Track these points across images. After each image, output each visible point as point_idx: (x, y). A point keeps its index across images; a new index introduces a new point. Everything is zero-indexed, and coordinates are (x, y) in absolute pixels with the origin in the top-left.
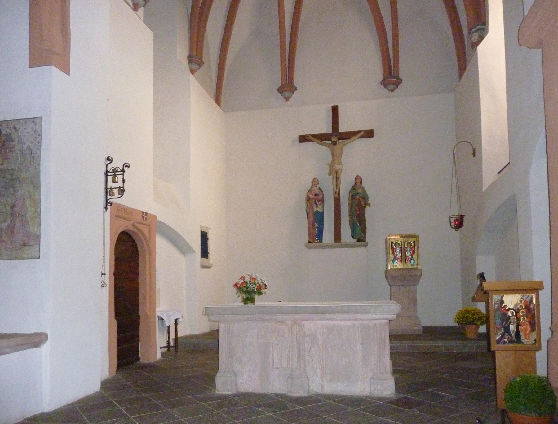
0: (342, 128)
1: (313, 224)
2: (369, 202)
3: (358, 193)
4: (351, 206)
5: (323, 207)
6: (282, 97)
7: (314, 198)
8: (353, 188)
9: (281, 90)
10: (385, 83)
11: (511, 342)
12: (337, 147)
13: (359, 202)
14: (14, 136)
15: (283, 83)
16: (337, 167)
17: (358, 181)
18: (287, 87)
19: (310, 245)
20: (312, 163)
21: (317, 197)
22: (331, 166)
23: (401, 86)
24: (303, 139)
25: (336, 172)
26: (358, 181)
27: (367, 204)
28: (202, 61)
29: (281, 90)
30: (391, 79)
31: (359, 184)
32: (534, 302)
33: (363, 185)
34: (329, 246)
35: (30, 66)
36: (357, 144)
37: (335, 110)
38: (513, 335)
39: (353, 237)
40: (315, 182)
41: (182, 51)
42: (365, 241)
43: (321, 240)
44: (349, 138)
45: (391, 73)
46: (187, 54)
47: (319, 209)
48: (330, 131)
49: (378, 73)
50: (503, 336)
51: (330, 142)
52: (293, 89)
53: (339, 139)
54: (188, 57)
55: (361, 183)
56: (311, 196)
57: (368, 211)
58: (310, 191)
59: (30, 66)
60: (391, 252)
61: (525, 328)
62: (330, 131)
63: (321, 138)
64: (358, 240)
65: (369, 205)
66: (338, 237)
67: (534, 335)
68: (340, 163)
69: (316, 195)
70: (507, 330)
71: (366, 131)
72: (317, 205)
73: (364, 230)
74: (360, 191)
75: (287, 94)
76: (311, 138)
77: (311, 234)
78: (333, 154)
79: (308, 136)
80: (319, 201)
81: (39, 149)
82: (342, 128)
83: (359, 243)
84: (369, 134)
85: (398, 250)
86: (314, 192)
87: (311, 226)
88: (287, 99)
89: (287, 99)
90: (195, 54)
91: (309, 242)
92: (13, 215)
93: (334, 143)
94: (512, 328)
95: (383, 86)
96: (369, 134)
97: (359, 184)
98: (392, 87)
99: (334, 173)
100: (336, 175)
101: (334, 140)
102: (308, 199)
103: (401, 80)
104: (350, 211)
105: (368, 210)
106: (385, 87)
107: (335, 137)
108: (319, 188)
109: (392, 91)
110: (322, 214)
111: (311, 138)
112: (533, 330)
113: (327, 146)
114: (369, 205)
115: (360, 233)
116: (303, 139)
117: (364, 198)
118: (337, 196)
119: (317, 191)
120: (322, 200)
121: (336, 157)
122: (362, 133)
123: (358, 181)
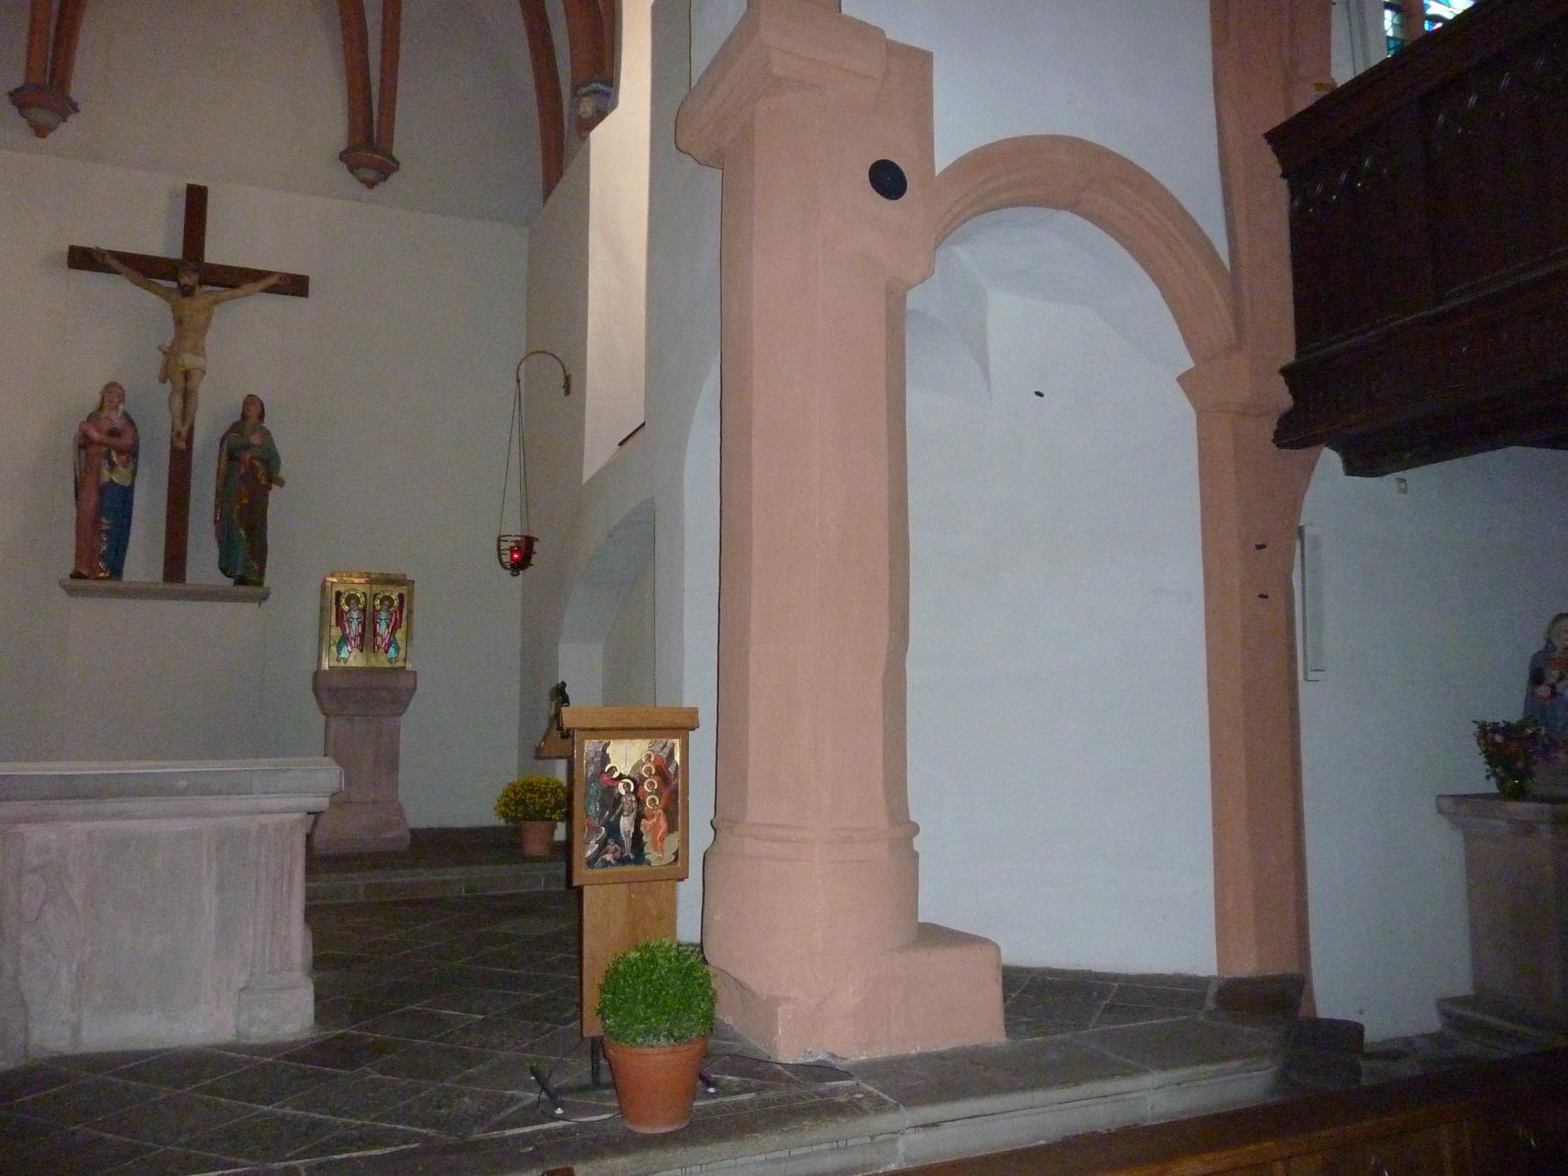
0: (217, 252)
1: (96, 522)
2: (282, 474)
3: (249, 447)
4: (224, 479)
5: (134, 474)
6: (24, 122)
7: (103, 443)
8: (236, 428)
9: (20, 100)
10: (351, 158)
11: (622, 861)
13: (250, 468)
16: (188, 360)
17: (253, 410)
19: (81, 583)
20: (112, 338)
21: (115, 441)
22: (170, 354)
23: (394, 178)
24: (82, 259)
25: (187, 375)
26: (254, 411)
27: (273, 479)
30: (369, 153)
31: (253, 420)
32: (677, 758)
33: (267, 423)
34: (140, 592)
36: (259, 307)
38: (628, 843)
39: (224, 570)
40: (112, 393)
42: (260, 584)
43: (116, 571)
44: (233, 286)
47: (120, 477)
48: (176, 252)
49: (334, 129)
50: (603, 845)
51: (174, 285)
53: (203, 282)
55: (261, 417)
56: (95, 435)
58: (93, 418)
60: (334, 622)
61: (655, 823)
62: (176, 252)
63: (143, 268)
64: (241, 581)
65: (281, 483)
67: (673, 842)
68: (199, 351)
69: (114, 433)
70: (613, 830)
72: (112, 466)
73: (258, 552)
74: (255, 439)
78: (179, 322)
80: (120, 452)
82: (217, 252)
83: (242, 589)
84: (296, 286)
85: (355, 615)
86: (106, 425)
87: (85, 531)
88: (41, 131)
91: (76, 575)
93: (187, 292)
94: (626, 824)
96: (296, 286)
97: (253, 420)
98: (370, 175)
99: (180, 379)
100: (183, 385)
101: (185, 280)
102: (84, 443)
103: (398, 163)
104: (221, 496)
105: (275, 496)
106: (352, 169)
107: (188, 273)
108: (126, 416)
109: (371, 185)
110: (127, 493)
112: (672, 828)
113: (166, 295)
114: (281, 483)
115: (245, 561)
116: (82, 259)
117: (266, 462)
118: (182, 445)
120: (132, 453)
121: (187, 333)
122: (272, 281)
123: (253, 410)
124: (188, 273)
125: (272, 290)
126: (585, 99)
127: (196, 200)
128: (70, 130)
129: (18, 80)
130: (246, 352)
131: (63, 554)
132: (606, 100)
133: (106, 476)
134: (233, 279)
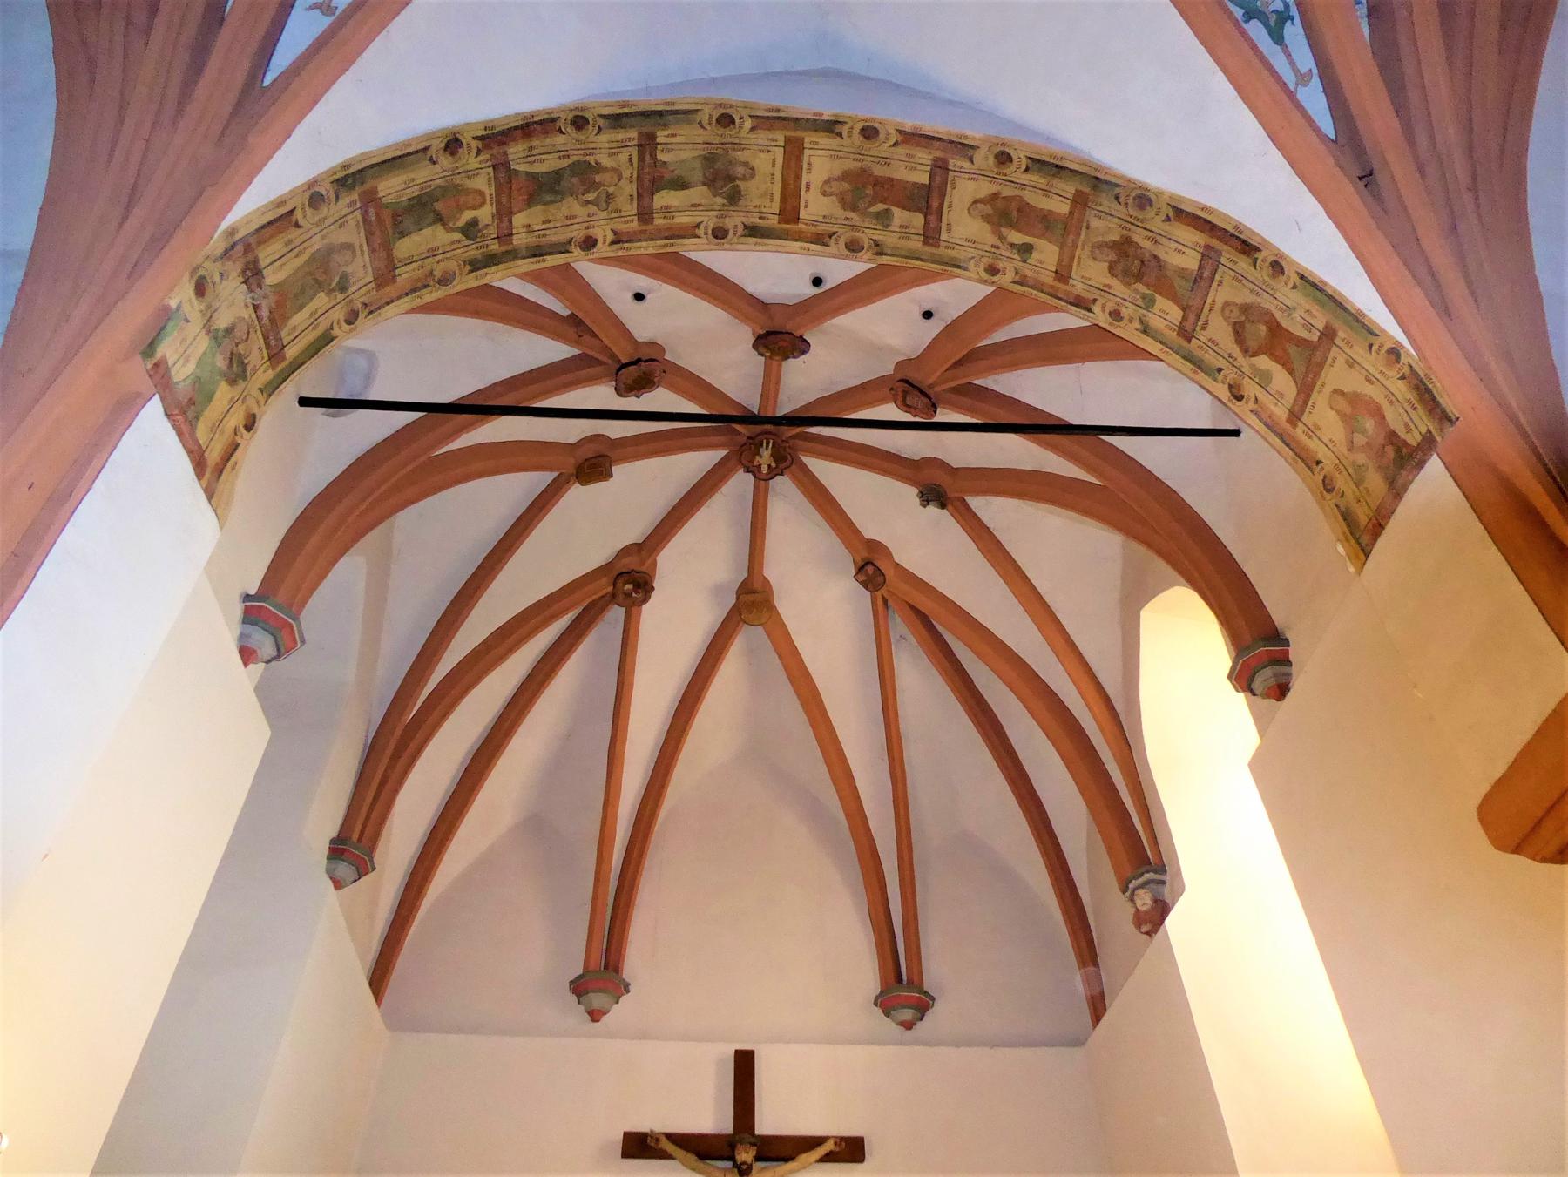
0: (768, 1122)
9: (579, 988)
10: (885, 1003)
15: (592, 966)
23: (929, 1016)
28: (372, 861)
29: (579, 988)
30: (903, 992)
37: (744, 1064)
41: (324, 817)
45: (899, 980)
46: (334, 834)
49: (866, 976)
51: (729, 1164)
52: (620, 989)
53: (758, 1158)
54: (333, 841)
63: (698, 1147)
71: (842, 1139)
76: (667, 1145)
79: (656, 1137)
82: (768, 1122)
88: (595, 1015)
89: (595, 1015)
90: (355, 836)
95: (878, 1011)
96: (852, 1150)
98: (907, 1014)
106: (887, 1014)
109: (908, 1026)
111: (667, 1145)
122: (829, 1147)
125: (829, 1158)
126: (1141, 892)
127: (744, 1064)
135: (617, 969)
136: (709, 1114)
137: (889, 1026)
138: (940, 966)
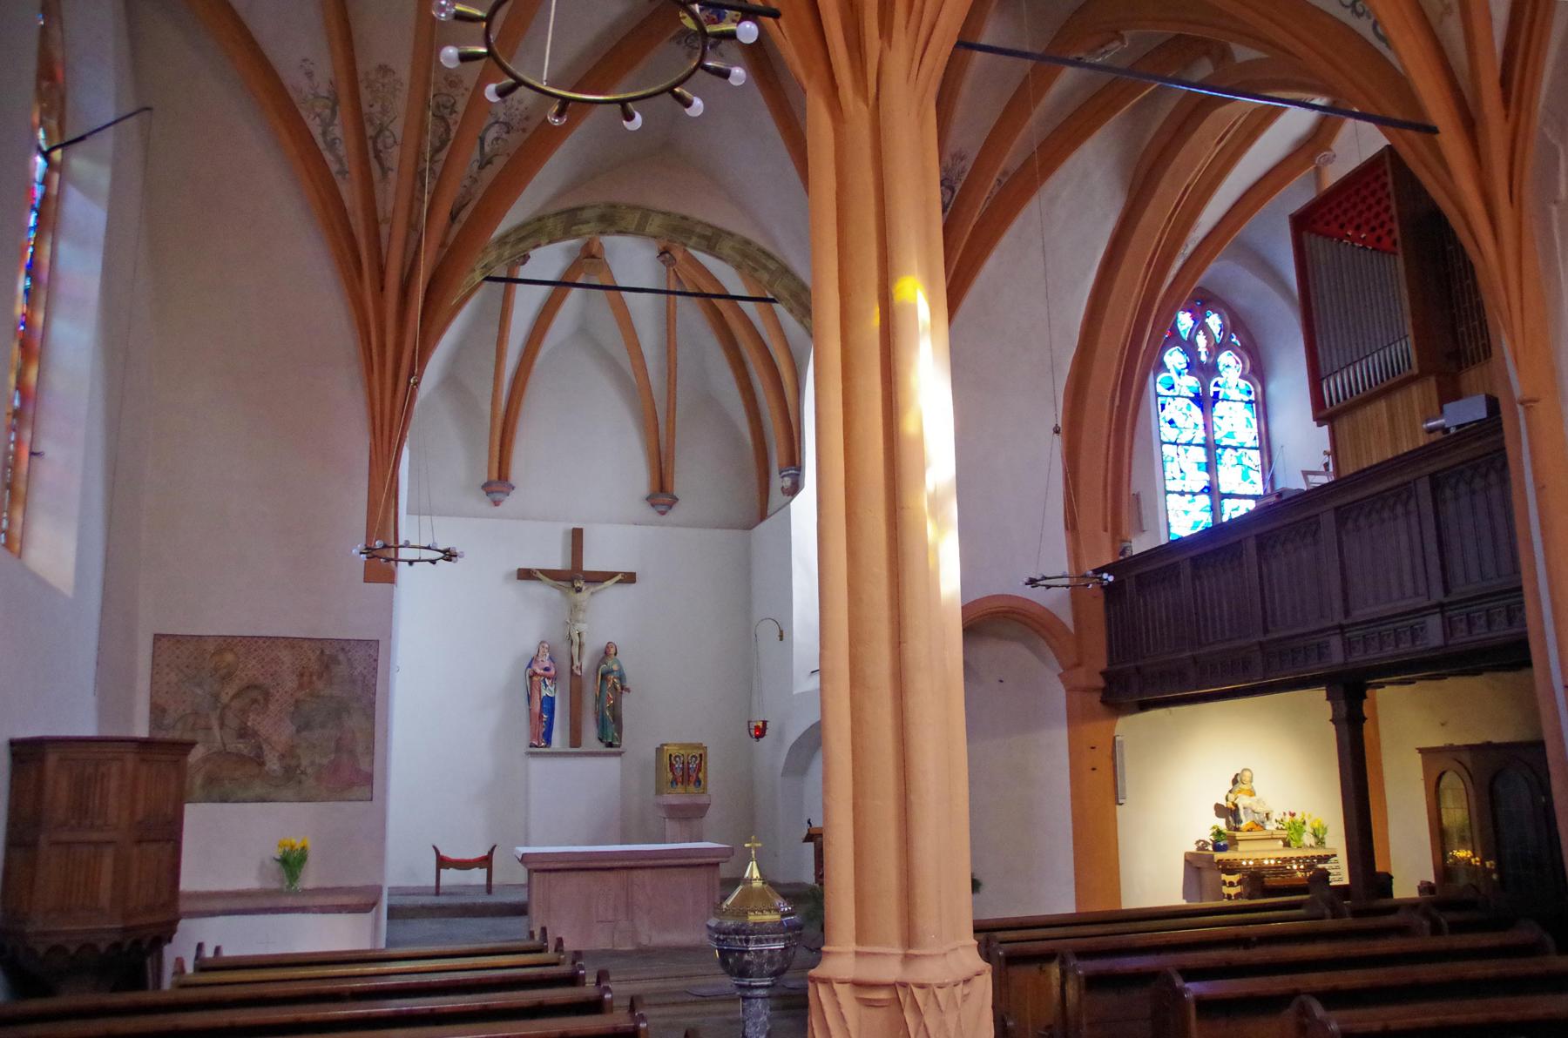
0: (588, 566)
9: (488, 488)
10: (652, 500)
12: (585, 595)
14: (341, 657)
17: (608, 652)
18: (498, 483)
23: (675, 507)
24: (526, 575)
29: (488, 488)
30: (662, 494)
35: (366, 580)
36: (611, 593)
43: (549, 742)
49: (641, 481)
56: (539, 671)
57: (628, 703)
59: (366, 580)
63: (553, 575)
64: (610, 745)
65: (628, 690)
66: (575, 739)
69: (546, 669)
74: (615, 667)
75: (498, 497)
77: (534, 735)
81: (375, 676)
84: (630, 578)
88: (496, 503)
92: (338, 749)
96: (630, 578)
105: (626, 700)
107: (574, 577)
110: (552, 699)
115: (611, 734)
119: (547, 665)
121: (574, 608)
124: (574, 577)
127: (577, 535)
128: (510, 502)
129: (485, 479)
130: (606, 619)
131: (522, 731)
132: (795, 489)
133: (544, 693)
134: (599, 578)
135: (506, 479)
136: (557, 560)
137: (651, 513)
138: (684, 481)
